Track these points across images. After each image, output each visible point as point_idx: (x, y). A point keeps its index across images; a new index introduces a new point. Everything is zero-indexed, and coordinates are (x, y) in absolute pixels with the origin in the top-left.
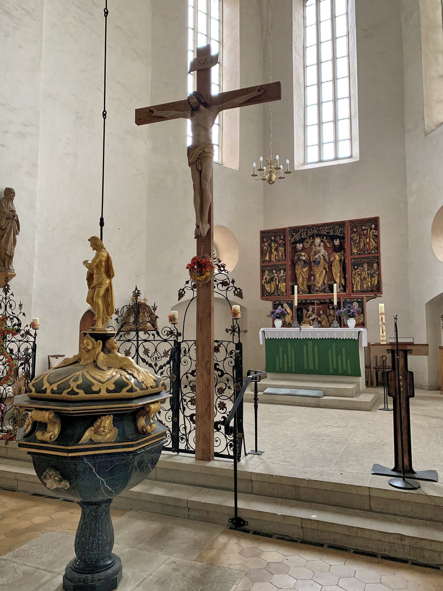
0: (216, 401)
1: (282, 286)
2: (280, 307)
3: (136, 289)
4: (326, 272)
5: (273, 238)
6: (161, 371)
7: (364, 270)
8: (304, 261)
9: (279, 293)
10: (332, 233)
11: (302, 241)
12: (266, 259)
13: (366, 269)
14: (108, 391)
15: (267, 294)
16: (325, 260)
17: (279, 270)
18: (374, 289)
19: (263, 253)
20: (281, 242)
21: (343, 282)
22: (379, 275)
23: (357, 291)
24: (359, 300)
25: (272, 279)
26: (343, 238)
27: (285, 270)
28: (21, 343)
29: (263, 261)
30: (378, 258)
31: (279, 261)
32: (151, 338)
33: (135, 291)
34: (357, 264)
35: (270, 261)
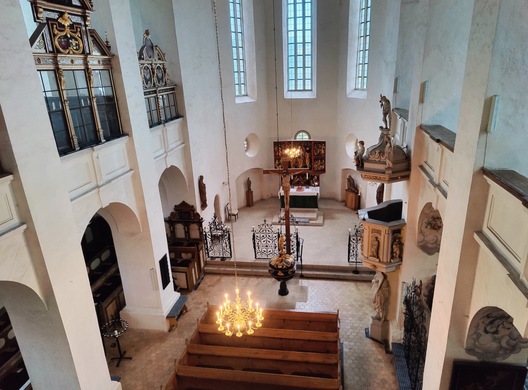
0: (291, 248)
4: (303, 161)
5: (280, 145)
7: (319, 162)
10: (306, 145)
16: (303, 156)
18: (323, 170)
19: (275, 152)
21: (310, 166)
22: (325, 165)
29: (275, 156)
30: (325, 158)
34: (316, 159)
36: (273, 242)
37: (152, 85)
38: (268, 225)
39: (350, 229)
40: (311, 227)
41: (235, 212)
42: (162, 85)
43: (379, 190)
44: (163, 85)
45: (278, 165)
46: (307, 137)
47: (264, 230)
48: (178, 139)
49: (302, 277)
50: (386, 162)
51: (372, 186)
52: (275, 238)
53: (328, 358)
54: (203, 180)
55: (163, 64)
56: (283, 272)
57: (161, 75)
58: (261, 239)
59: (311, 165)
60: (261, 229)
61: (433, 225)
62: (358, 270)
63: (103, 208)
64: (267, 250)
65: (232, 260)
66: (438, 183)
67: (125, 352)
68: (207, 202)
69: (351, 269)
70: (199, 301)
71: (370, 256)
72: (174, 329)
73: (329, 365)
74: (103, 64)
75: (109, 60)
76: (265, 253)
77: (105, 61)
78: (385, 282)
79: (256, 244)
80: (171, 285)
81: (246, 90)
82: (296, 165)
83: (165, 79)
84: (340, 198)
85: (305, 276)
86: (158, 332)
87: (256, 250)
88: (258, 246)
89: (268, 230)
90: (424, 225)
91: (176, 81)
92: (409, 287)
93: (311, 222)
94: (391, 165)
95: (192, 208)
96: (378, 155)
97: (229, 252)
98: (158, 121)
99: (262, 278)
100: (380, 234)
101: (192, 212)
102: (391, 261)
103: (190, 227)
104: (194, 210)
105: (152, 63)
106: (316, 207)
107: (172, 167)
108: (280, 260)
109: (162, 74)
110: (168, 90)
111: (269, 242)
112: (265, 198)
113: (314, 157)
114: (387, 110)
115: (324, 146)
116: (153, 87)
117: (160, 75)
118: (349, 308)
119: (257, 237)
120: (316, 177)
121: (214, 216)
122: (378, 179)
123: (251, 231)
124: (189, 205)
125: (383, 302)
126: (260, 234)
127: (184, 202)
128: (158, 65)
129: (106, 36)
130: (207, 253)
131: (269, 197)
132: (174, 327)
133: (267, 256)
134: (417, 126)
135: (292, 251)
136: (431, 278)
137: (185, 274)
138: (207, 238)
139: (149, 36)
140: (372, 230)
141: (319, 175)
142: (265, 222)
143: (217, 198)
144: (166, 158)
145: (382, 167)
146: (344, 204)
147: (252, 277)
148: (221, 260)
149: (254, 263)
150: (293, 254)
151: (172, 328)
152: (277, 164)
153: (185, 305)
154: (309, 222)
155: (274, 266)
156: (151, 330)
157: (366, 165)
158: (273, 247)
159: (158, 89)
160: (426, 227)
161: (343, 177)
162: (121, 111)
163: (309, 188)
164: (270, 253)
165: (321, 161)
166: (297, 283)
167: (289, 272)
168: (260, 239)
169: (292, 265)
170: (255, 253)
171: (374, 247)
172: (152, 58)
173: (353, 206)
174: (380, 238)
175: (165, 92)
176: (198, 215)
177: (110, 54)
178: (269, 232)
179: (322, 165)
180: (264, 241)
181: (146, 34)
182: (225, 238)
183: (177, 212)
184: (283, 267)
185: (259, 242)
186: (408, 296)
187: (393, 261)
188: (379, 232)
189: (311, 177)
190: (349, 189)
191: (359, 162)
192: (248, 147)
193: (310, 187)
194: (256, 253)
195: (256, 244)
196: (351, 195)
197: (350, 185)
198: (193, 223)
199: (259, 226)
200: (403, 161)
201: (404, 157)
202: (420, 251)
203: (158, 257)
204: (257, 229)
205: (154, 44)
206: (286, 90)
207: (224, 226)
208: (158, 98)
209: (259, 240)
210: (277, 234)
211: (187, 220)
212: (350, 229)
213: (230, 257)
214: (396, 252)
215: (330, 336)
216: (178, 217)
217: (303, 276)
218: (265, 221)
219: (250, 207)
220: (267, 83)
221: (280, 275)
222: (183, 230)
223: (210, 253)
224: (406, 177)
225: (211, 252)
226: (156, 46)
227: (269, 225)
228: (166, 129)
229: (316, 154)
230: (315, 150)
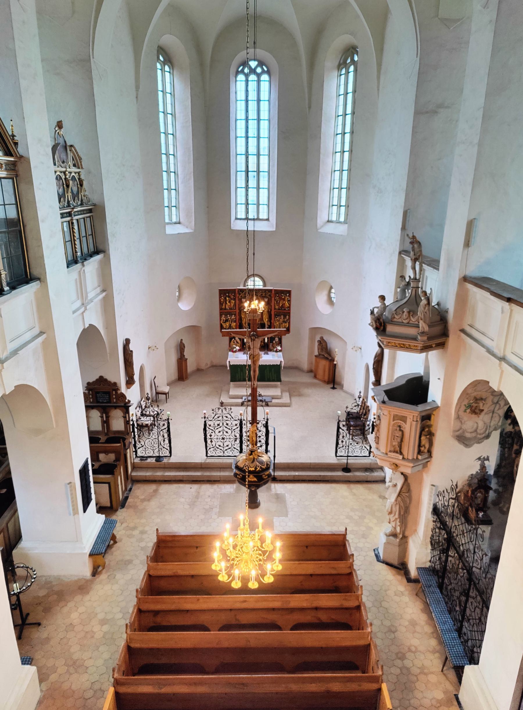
1: (234, 324)
2: (233, 339)
5: (227, 294)
13: (282, 318)
17: (231, 315)
19: (221, 304)
20: (232, 297)
21: (269, 324)
22: (289, 323)
25: (227, 321)
27: (235, 315)
29: (221, 309)
30: (289, 313)
31: (231, 309)
35: (225, 309)
37: (66, 204)
39: (339, 412)
40: (275, 408)
41: (166, 389)
42: (77, 203)
43: (376, 358)
44: (79, 204)
45: (225, 322)
46: (261, 283)
48: (96, 285)
49: (275, 480)
50: (419, 325)
51: (355, 352)
52: (236, 427)
53: (345, 599)
54: (130, 345)
55: (79, 173)
56: (255, 476)
57: (76, 189)
59: (271, 323)
61: (473, 408)
62: (349, 467)
63: (7, 393)
65: (173, 459)
66: (502, 355)
67: (28, 614)
69: (340, 465)
70: (132, 525)
71: (390, 451)
72: (100, 571)
73: (347, 609)
74: (6, 170)
75: (14, 164)
76: (220, 448)
77: (9, 164)
78: (405, 487)
80: (93, 506)
83: (81, 195)
84: (305, 366)
85: (278, 479)
86: (76, 578)
87: (208, 445)
89: (226, 415)
90: (463, 408)
91: (95, 199)
92: (444, 491)
93: (274, 401)
94: (426, 329)
95: (115, 386)
96: (407, 315)
97: (167, 449)
98: (72, 259)
99: (218, 485)
100: (405, 422)
101: (114, 392)
102: (418, 458)
103: (110, 414)
104: (117, 388)
105: (66, 171)
106: (279, 380)
107: (91, 326)
108: (250, 459)
109: (78, 187)
110: (85, 212)
111: (227, 432)
112: (202, 368)
114: (418, 255)
116: (67, 206)
117: (75, 189)
118: (347, 521)
119: (210, 425)
120: (277, 339)
122: (407, 348)
124: (110, 382)
125: (402, 513)
126: (214, 421)
127: (101, 377)
128: (73, 174)
129: (12, 126)
130: (134, 452)
131: (208, 366)
132: (100, 569)
134: (460, 278)
135: (259, 445)
136: (467, 478)
137: (107, 485)
139: (62, 130)
140: (394, 417)
141: (281, 337)
143: (142, 369)
144: (84, 313)
145: (412, 331)
146: (313, 374)
147: (203, 483)
148: (156, 461)
150: (260, 448)
151: (96, 571)
152: (223, 320)
153: (113, 534)
154: (271, 402)
155: (243, 468)
156: (64, 576)
157: (390, 328)
158: (232, 440)
159: (75, 210)
160: (465, 411)
161: (312, 339)
162: (30, 243)
163: (268, 354)
164: (227, 448)
165: (285, 317)
166: (269, 489)
167: (264, 476)
169: (268, 466)
171: (397, 439)
172: (65, 164)
173: (326, 378)
174: (405, 427)
175: (81, 214)
176: (123, 396)
177: (18, 155)
178: (227, 419)
179: (285, 323)
180: (219, 432)
181: (58, 126)
182: (162, 429)
183: (91, 392)
184: (256, 468)
185: (212, 433)
186: (440, 505)
187: (421, 457)
188: (404, 419)
190: (320, 355)
191: (381, 324)
192: (180, 296)
193: (269, 353)
194: (208, 449)
195: (208, 437)
196: (323, 364)
197: (322, 349)
198: (116, 409)
199: (213, 410)
200: (438, 323)
201: (438, 318)
202: (456, 443)
203: (78, 466)
204: (210, 414)
205: (68, 144)
207: (161, 412)
208: (72, 223)
209: (212, 430)
210: (239, 421)
211: (107, 405)
212: (339, 412)
213: (169, 455)
214: (424, 445)
215: (340, 567)
216: (91, 400)
217: (276, 478)
219: (184, 381)
222: (100, 419)
223: (139, 451)
224: (442, 345)
225: (141, 449)
226: (71, 146)
227: (227, 409)
228: (84, 270)
229: (277, 307)
230: (277, 302)
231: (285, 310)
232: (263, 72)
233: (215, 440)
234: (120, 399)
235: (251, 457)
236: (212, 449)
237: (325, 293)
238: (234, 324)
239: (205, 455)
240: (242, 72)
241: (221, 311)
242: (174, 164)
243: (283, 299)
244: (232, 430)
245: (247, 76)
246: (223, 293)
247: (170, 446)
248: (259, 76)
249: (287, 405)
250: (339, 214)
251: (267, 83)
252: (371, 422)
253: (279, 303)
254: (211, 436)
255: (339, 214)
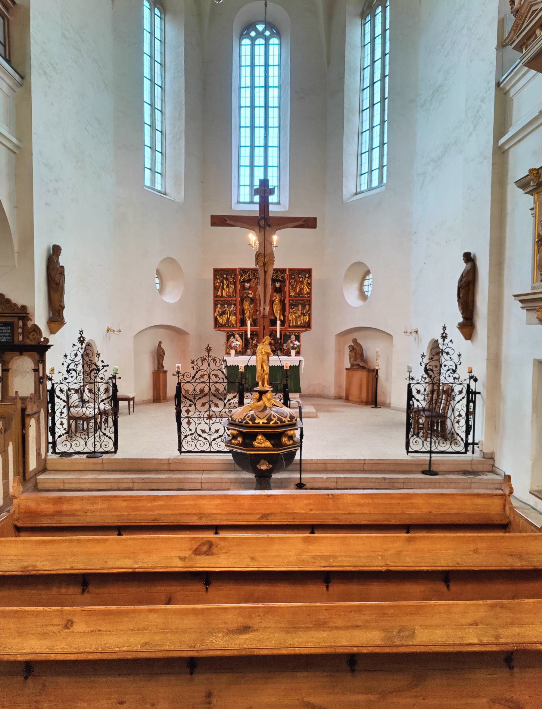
1: (233, 319)
2: (232, 337)
3: (208, 346)
5: (225, 276)
6: (229, 402)
7: (298, 310)
8: (251, 298)
9: (230, 325)
11: (249, 281)
12: (218, 294)
13: (300, 309)
14: (288, 421)
15: (220, 325)
17: (230, 305)
19: (216, 289)
20: (231, 280)
21: (282, 318)
22: (310, 315)
23: (293, 327)
24: (296, 334)
25: (223, 313)
26: (284, 282)
27: (235, 305)
28: (100, 384)
29: (216, 296)
30: (310, 301)
31: (230, 296)
32: (221, 381)
33: (207, 348)
34: (293, 305)
35: (222, 296)
36: (225, 405)
38: (214, 360)
43: (464, 279)
47: (206, 373)
54: (60, 257)
58: (197, 398)
60: (197, 372)
64: (210, 429)
65: (119, 455)
68: (65, 313)
76: (204, 435)
79: (184, 410)
81: (163, 184)
82: (254, 317)
87: (182, 429)
88: (187, 417)
89: (216, 373)
97: (110, 438)
101: (21, 323)
113: (290, 299)
115: (308, 278)
119: (187, 391)
121: (79, 338)
123: (173, 375)
124: (15, 305)
126: (196, 384)
133: (210, 444)
138: (56, 400)
142: (209, 353)
149: (177, 462)
152: (219, 312)
165: (304, 307)
168: (195, 399)
170: (180, 436)
173: (364, 396)
178: (217, 380)
179: (305, 315)
185: (190, 406)
189: (286, 337)
190: (352, 365)
194: (183, 437)
195: (184, 414)
198: (21, 354)
199: (193, 362)
206: (234, 200)
209: (191, 401)
213: (113, 450)
218: (209, 350)
220: (202, 182)
221: (261, 448)
227: (218, 360)
231: (303, 297)
232: (272, 35)
233: (195, 420)
234: (31, 336)
235: (261, 403)
236: (190, 436)
237: (355, 286)
238: (233, 319)
239: (177, 448)
240: (248, 36)
241: (216, 299)
242: (162, 122)
243: (300, 282)
244: (226, 401)
245: (253, 40)
246: (218, 273)
247: (116, 432)
248: (267, 39)
249: (311, 415)
250: (370, 181)
251: (277, 48)
252: (466, 386)
253: (296, 288)
254: (188, 411)
255: (370, 181)
